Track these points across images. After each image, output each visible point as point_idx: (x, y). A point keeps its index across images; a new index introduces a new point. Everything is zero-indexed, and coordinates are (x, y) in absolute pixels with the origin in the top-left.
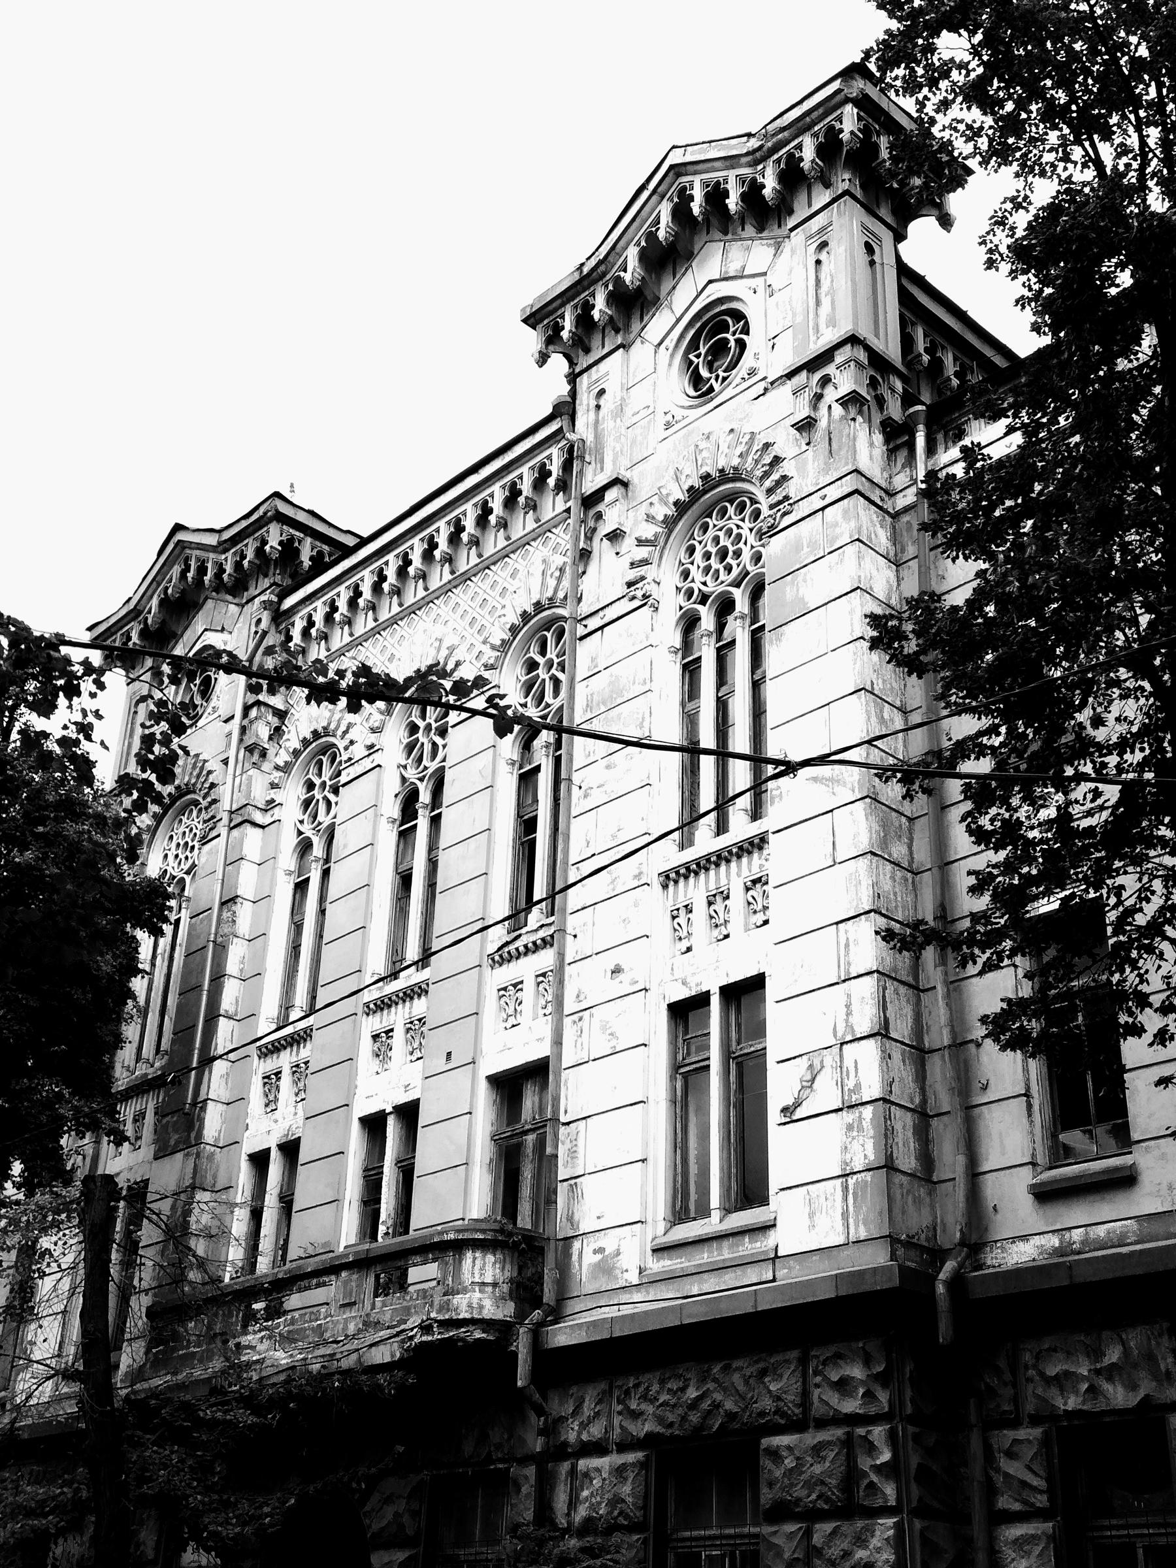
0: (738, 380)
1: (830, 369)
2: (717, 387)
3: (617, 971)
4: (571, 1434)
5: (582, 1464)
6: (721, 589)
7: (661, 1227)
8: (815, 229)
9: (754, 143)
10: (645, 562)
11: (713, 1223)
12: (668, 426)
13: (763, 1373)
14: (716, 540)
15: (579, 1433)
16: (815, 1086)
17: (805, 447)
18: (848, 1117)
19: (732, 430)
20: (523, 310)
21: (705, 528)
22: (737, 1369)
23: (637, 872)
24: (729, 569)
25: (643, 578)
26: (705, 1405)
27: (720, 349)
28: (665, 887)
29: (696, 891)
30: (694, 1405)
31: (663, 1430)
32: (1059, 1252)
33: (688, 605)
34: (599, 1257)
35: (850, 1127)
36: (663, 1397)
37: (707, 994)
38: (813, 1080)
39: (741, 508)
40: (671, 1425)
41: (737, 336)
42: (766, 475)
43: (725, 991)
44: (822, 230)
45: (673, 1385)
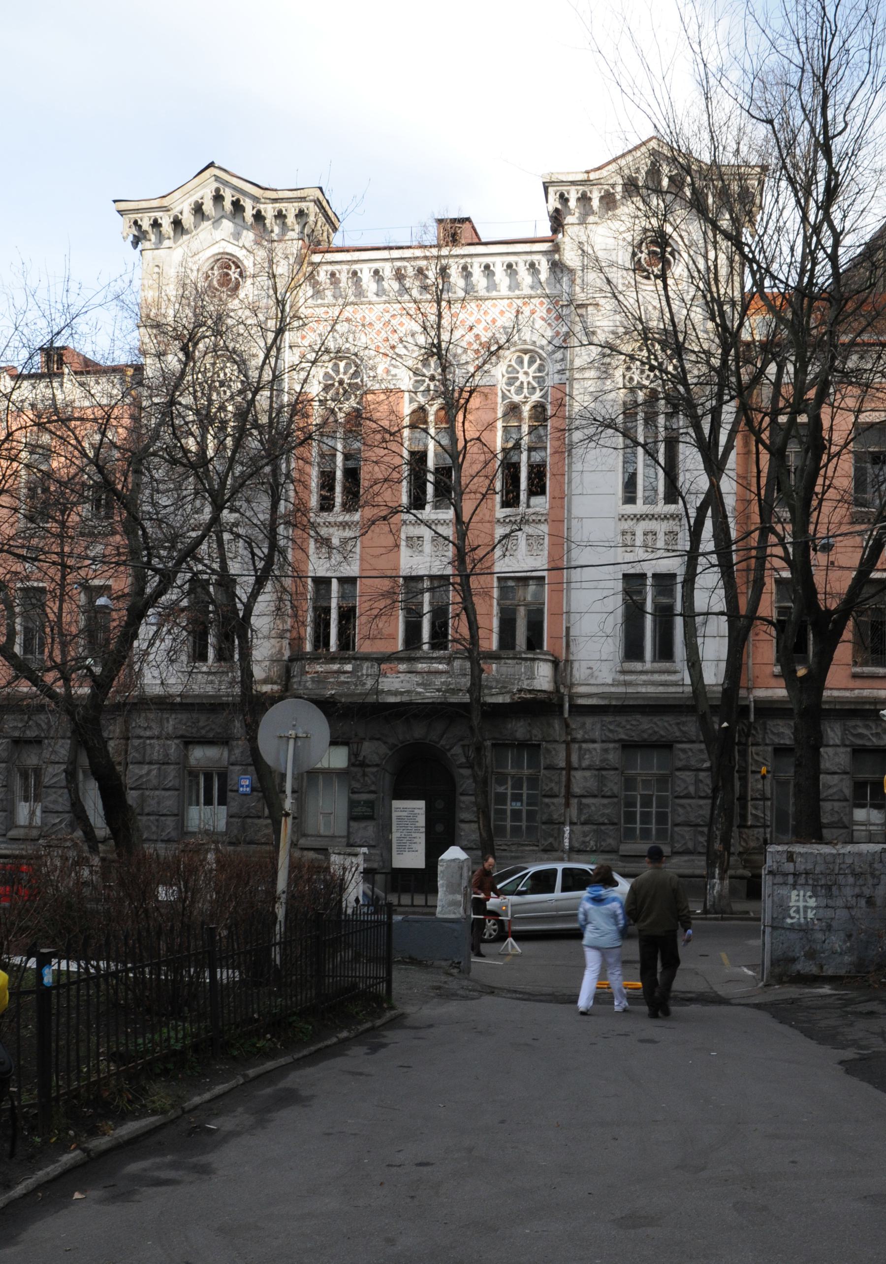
5: (584, 746)
11: (648, 665)
26: (650, 731)
36: (628, 727)
37: (643, 576)
45: (634, 723)
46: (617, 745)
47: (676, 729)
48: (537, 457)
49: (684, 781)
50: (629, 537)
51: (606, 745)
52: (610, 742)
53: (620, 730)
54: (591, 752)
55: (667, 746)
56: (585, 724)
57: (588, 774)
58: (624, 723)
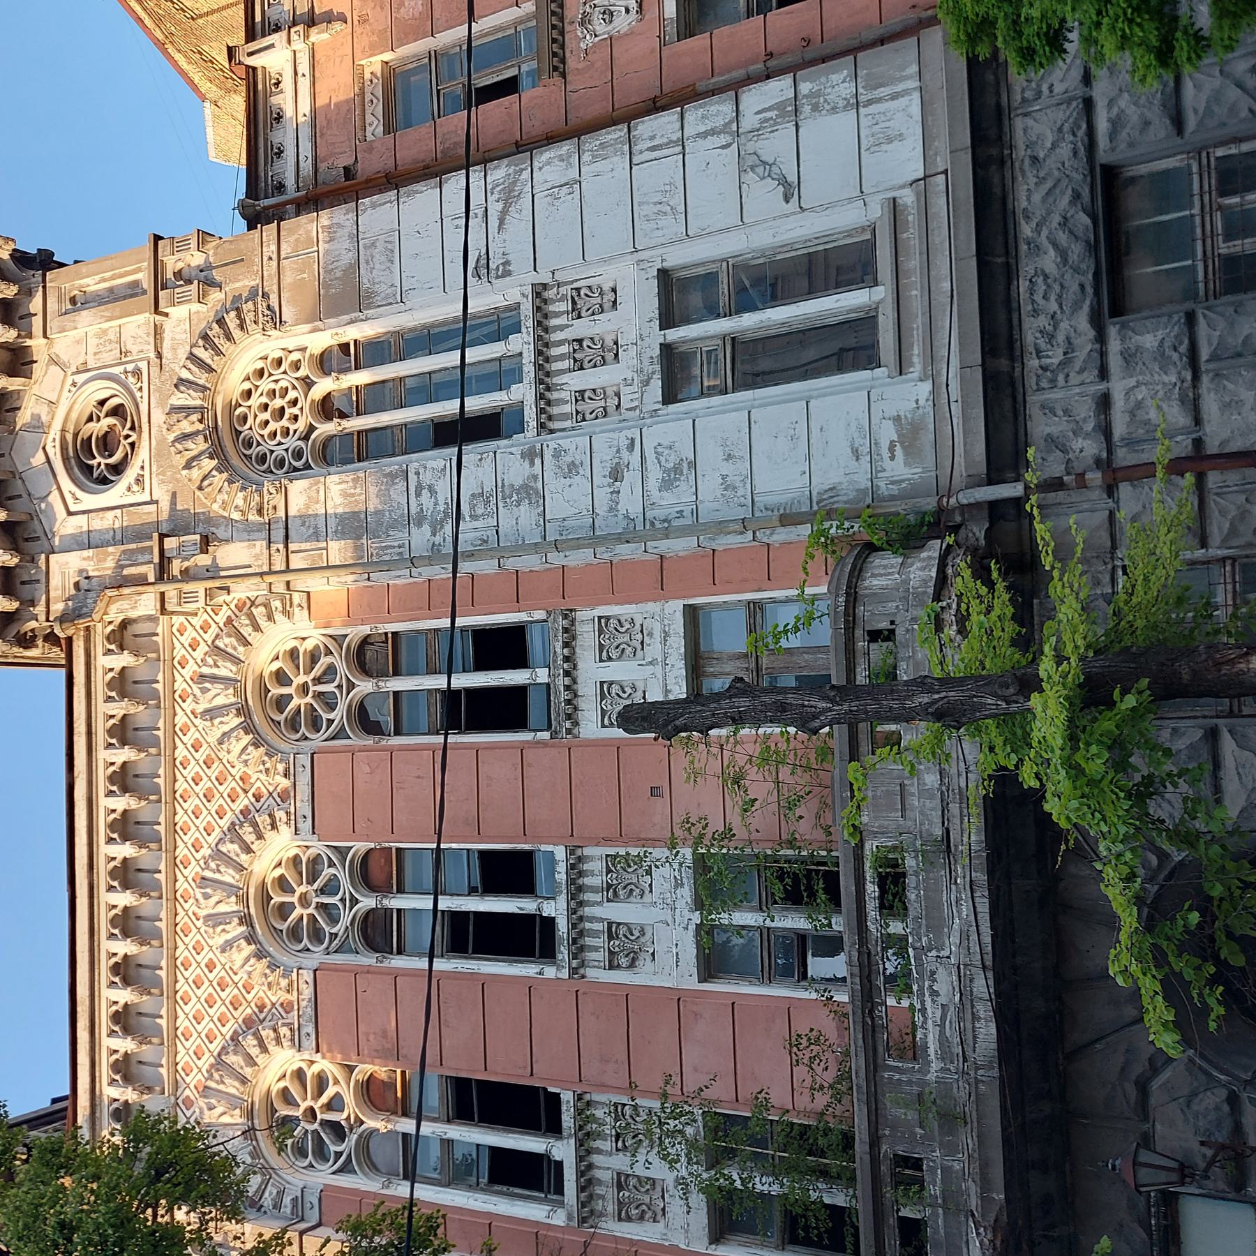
0: (138, 395)
2: (134, 438)
4: (1088, 448)
5: (1120, 428)
6: (306, 410)
13: (1035, 159)
15: (1087, 436)
19: (176, 386)
22: (1029, 200)
23: (527, 462)
26: (1063, 238)
28: (552, 432)
30: (1063, 254)
31: (1088, 302)
34: (899, 451)
35: (815, 108)
36: (1054, 306)
38: (765, 163)
39: (248, 394)
40: (1082, 286)
41: (102, 415)
43: (668, 319)
44: (60, 301)
46: (1113, 331)
47: (1051, 163)
49: (1217, 97)
50: (586, 407)
51: (1115, 362)
52: (1103, 354)
53: (1064, 325)
54: (1139, 405)
55: (1109, 185)
56: (1050, 439)
57: (1211, 405)
58: (1042, 321)
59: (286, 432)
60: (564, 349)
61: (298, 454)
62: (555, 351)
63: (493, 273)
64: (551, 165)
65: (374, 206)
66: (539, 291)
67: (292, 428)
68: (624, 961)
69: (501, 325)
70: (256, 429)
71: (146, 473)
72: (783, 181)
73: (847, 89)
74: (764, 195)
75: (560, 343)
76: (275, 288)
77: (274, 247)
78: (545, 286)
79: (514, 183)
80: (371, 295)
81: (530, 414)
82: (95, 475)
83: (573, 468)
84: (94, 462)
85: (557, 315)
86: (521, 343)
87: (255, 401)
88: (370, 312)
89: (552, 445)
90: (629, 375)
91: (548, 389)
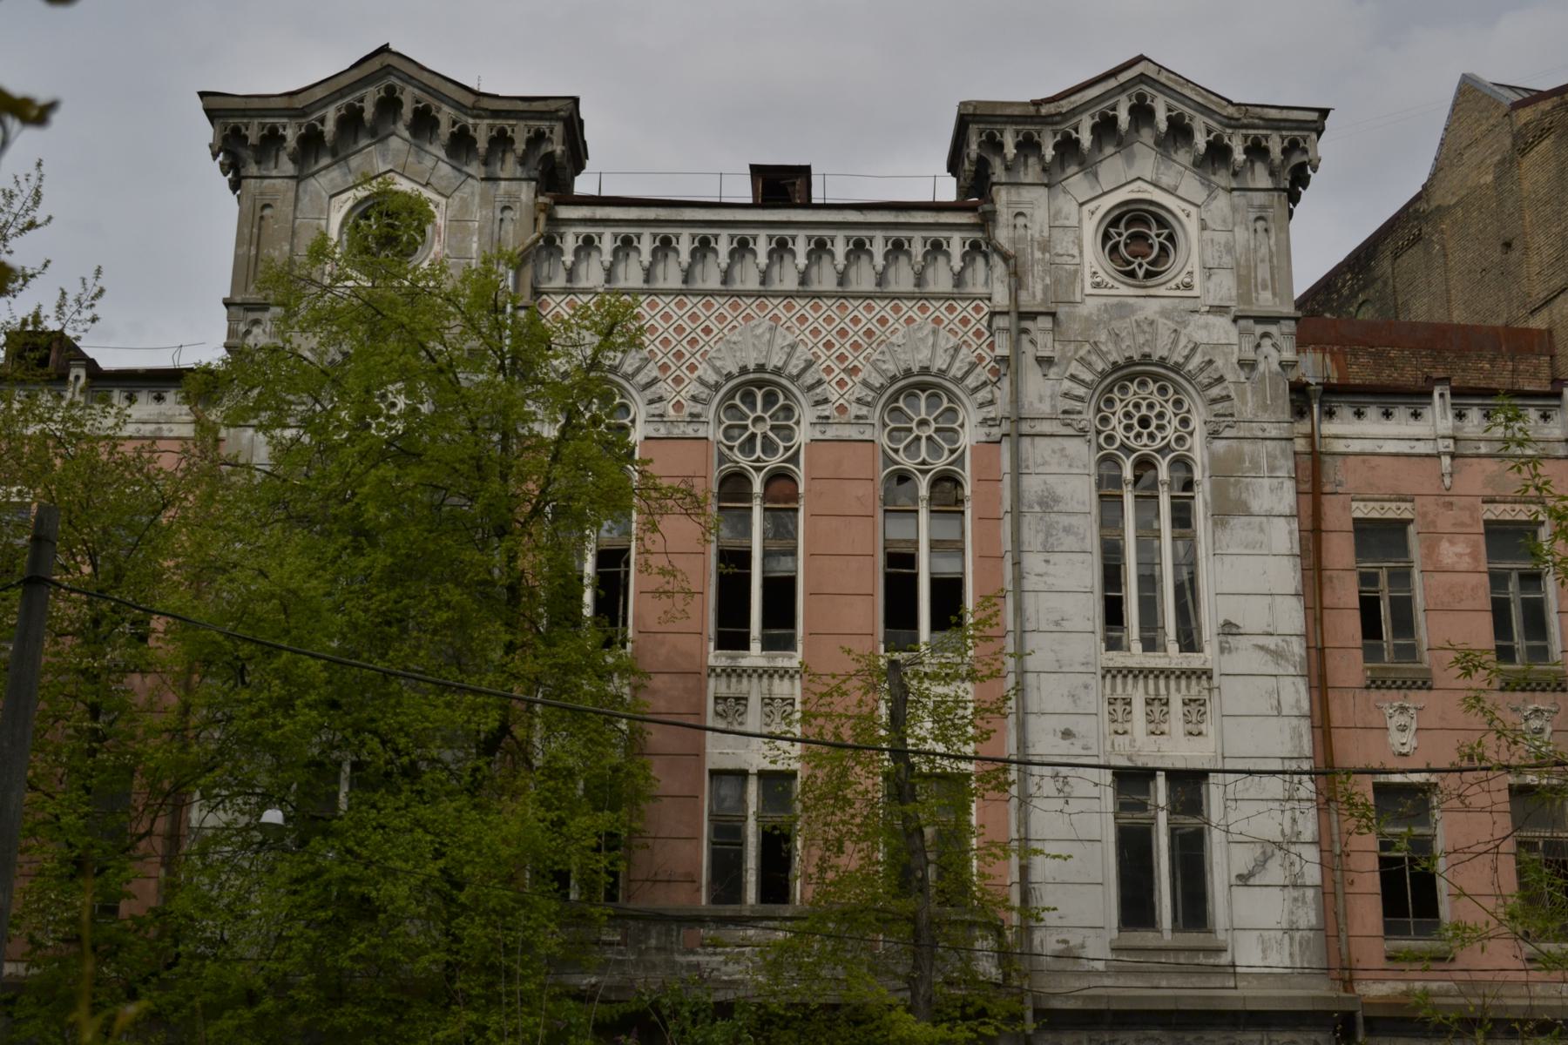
0: (1172, 284)
1: (1273, 329)
2: (1141, 273)
3: (1067, 734)
6: (1146, 451)
7: (1115, 934)
8: (1257, 202)
9: (1231, 110)
10: (1080, 399)
12: (1097, 285)
14: (1137, 406)
16: (1268, 865)
17: (1243, 379)
18: (1296, 893)
20: (963, 104)
21: (1124, 389)
24: (1151, 436)
25: (1080, 413)
27: (1145, 237)
28: (1104, 677)
29: (1138, 694)
32: (1406, 994)
33: (1111, 449)
34: (1062, 946)
35: (1295, 900)
39: (1163, 390)
42: (1210, 385)
43: (1174, 776)
44: (1262, 207)
48: (948, 567)
50: (1119, 707)
59: (1128, 428)
60: (1163, 691)
61: (1110, 439)
62: (1162, 682)
63: (1223, 638)
64: (1296, 693)
65: (1291, 533)
66: (1207, 674)
67: (1132, 435)
68: (720, 708)
69: (1189, 641)
70: (1135, 399)
71: (1106, 292)
72: (1251, 874)
73: (1303, 924)
74: (1243, 859)
75: (1167, 688)
76: (1241, 434)
77: (1274, 433)
78: (1210, 678)
79: (1287, 660)
80: (1224, 525)
81: (1118, 659)
82: (1112, 230)
83: (1074, 697)
84: (1122, 228)
85: (1188, 687)
86: (1172, 656)
87: (1156, 398)
88: (1210, 522)
89: (1093, 683)
90: (1138, 744)
91: (1135, 677)
